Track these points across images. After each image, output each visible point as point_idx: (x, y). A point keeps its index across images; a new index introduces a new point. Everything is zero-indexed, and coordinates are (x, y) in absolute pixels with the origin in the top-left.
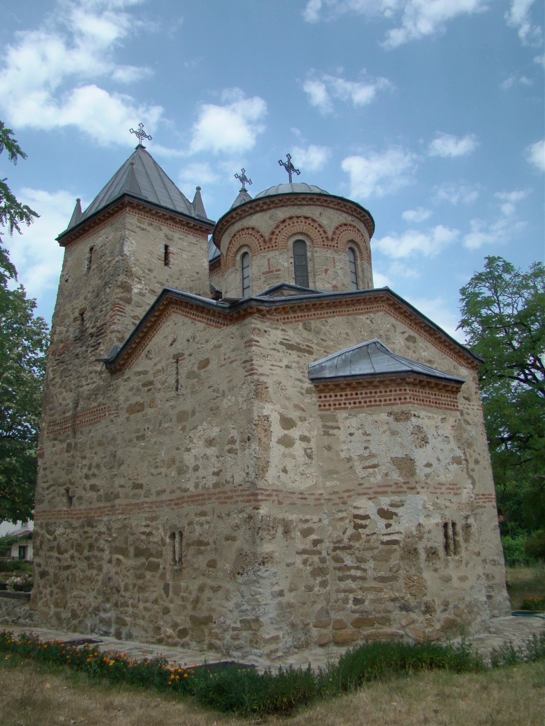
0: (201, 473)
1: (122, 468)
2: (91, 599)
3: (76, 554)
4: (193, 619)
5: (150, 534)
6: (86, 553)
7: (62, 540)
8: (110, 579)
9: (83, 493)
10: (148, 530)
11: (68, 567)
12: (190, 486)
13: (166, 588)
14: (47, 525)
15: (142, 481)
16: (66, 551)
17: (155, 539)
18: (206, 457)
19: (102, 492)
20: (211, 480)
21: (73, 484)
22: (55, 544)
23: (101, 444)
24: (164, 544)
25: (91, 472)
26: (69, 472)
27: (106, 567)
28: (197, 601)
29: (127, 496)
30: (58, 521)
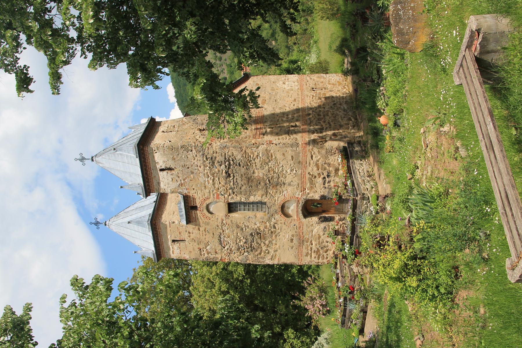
0: (293, 85)
1: (286, 105)
2: (341, 113)
3: (323, 120)
4: (339, 85)
5: (313, 96)
6: (322, 117)
8: (331, 107)
10: (311, 97)
11: (329, 123)
12: (297, 88)
13: (331, 91)
16: (322, 126)
20: (296, 84)
25: (286, 117)
27: (326, 109)
28: (333, 84)
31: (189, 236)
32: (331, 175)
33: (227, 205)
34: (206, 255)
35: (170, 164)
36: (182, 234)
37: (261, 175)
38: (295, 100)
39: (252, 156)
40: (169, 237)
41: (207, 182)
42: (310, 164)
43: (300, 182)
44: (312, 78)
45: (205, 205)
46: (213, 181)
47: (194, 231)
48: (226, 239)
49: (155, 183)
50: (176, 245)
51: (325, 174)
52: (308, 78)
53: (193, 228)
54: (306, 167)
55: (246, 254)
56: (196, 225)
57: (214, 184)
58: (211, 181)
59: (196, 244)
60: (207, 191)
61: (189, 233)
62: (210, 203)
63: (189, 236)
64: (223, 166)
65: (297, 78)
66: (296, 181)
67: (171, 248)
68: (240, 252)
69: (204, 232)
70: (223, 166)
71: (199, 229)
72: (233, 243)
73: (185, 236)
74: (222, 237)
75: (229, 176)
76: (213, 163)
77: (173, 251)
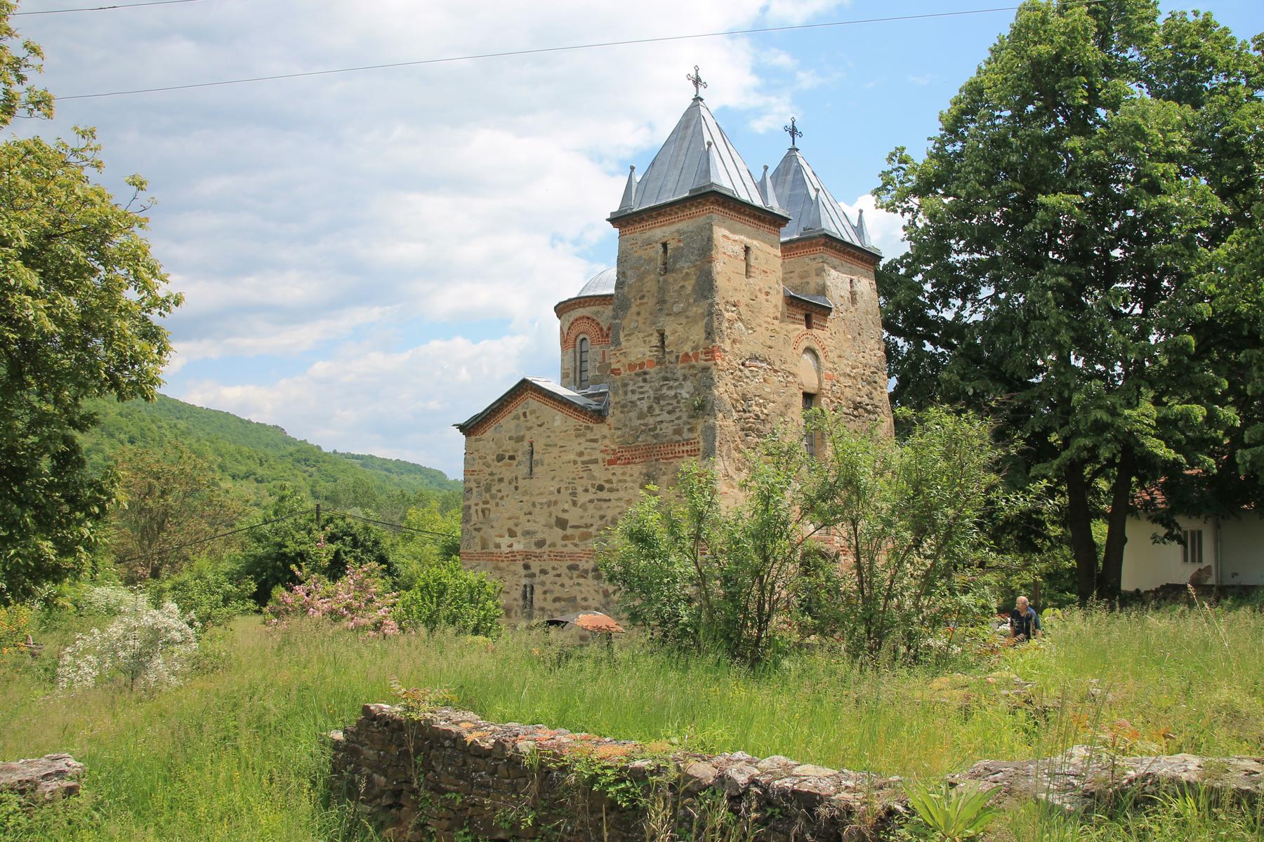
33: (812, 391)
34: (727, 315)
35: (861, 304)
40: (755, 242)
45: (816, 347)
48: (761, 372)
49: (836, 262)
55: (736, 415)
56: (782, 314)
58: (848, 370)
60: (836, 360)
61: (767, 294)
62: (817, 357)
64: (867, 401)
67: (731, 236)
68: (737, 401)
69: (771, 327)
70: (867, 401)
71: (776, 318)
72: (757, 389)
73: (758, 281)
74: (764, 365)
75: (856, 409)
76: (869, 383)
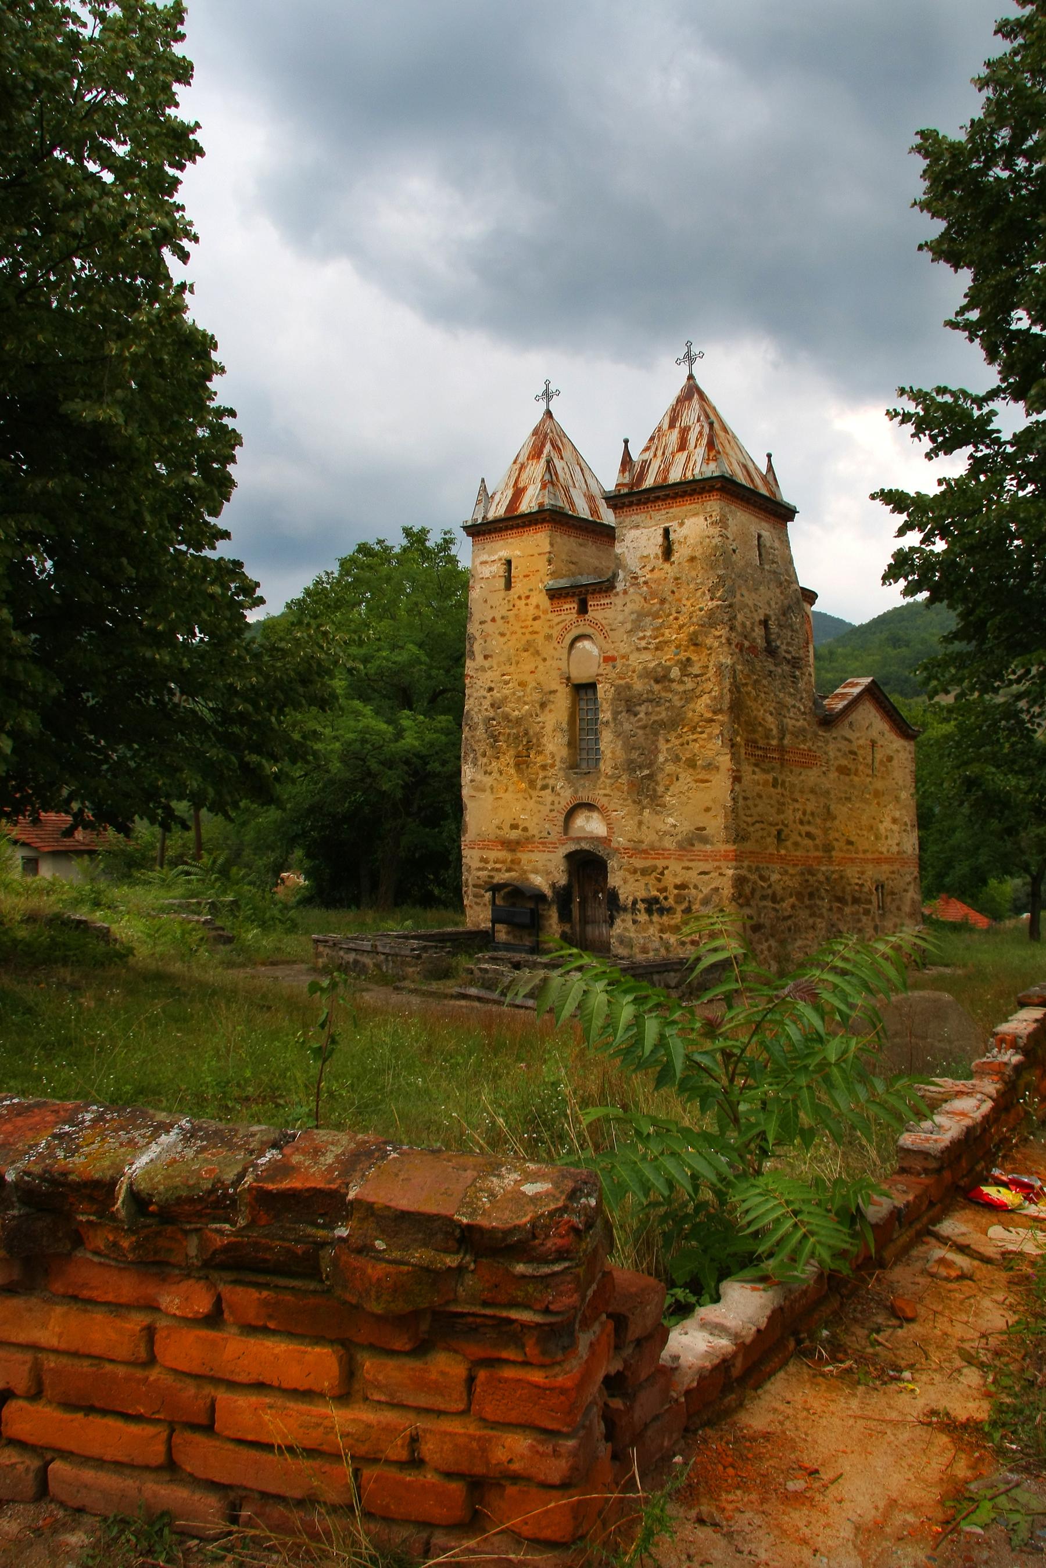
0: (889, 842)
6: (807, 902)
7: (778, 888)
9: (799, 839)
12: (884, 850)
14: (757, 869)
15: (852, 839)
16: (783, 900)
17: (866, 889)
18: (891, 830)
19: (817, 842)
20: (895, 849)
21: (786, 826)
22: (770, 891)
23: (812, 791)
24: (871, 894)
26: (780, 812)
29: (841, 850)
30: (770, 866)
31: (520, 598)
32: (665, 918)
36: (525, 580)
37: (661, 759)
38: (850, 843)
39: (704, 736)
41: (641, 634)
42: (688, 868)
43: (644, 846)
44: (912, 886)
45: (589, 631)
46: (646, 648)
47: (531, 608)
50: (499, 569)
51: (665, 904)
52: (908, 878)
53: (537, 607)
54: (680, 858)
57: (638, 649)
58: (643, 643)
59: (504, 612)
61: (528, 597)
63: (520, 598)
65: (910, 851)
66: (649, 837)
77: (486, 562)
